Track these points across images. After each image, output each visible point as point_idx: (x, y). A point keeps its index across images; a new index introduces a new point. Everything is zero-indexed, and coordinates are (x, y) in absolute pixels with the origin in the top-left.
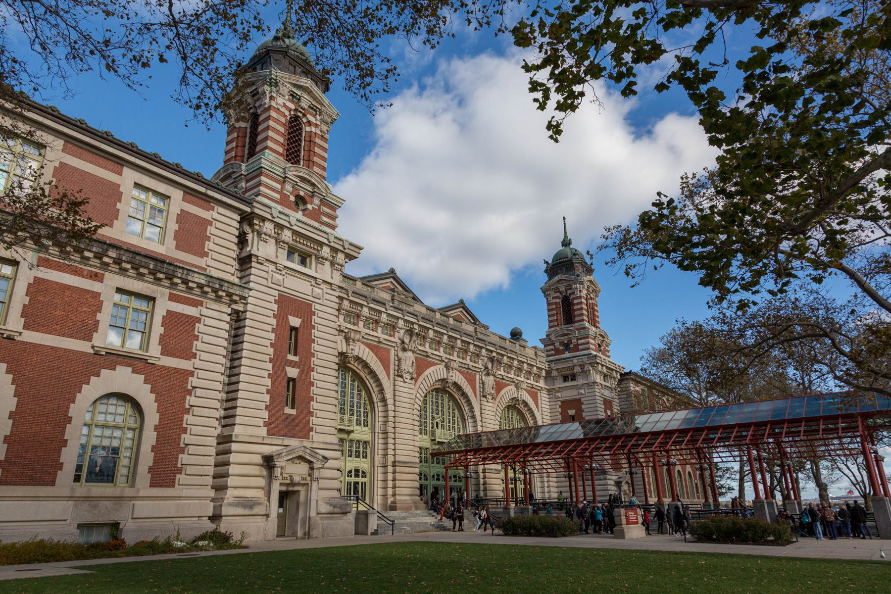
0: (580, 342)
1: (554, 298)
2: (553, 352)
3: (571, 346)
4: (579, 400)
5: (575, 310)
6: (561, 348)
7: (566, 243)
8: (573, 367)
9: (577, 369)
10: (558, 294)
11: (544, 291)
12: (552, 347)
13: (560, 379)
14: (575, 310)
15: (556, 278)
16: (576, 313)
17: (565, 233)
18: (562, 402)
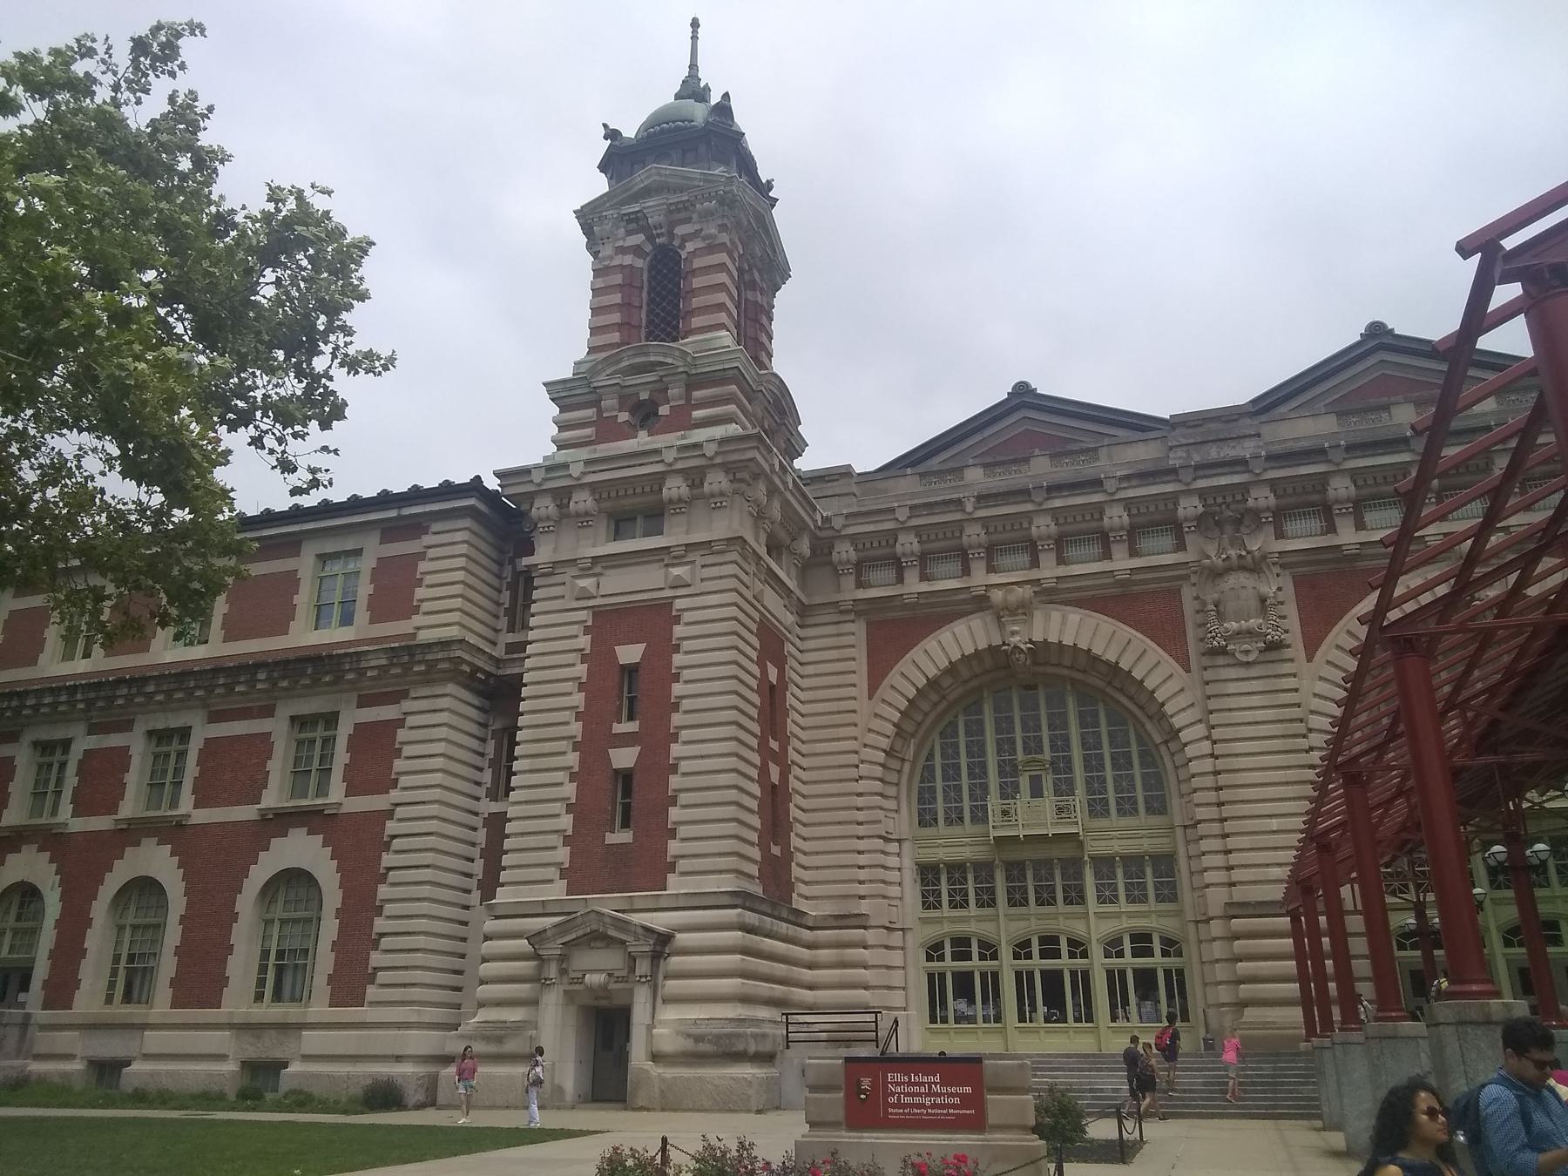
0: (697, 394)
1: (622, 250)
2: (588, 431)
3: (664, 410)
4: (667, 604)
5: (694, 292)
6: (624, 417)
7: (692, 89)
8: (660, 478)
9: (675, 488)
10: (638, 239)
11: (589, 217)
12: (589, 413)
13: (603, 527)
14: (694, 292)
15: (642, 177)
16: (696, 302)
17: (693, 66)
18: (597, 613)
